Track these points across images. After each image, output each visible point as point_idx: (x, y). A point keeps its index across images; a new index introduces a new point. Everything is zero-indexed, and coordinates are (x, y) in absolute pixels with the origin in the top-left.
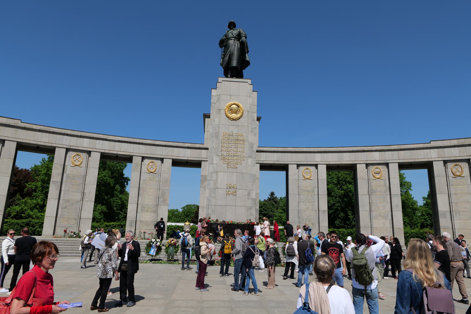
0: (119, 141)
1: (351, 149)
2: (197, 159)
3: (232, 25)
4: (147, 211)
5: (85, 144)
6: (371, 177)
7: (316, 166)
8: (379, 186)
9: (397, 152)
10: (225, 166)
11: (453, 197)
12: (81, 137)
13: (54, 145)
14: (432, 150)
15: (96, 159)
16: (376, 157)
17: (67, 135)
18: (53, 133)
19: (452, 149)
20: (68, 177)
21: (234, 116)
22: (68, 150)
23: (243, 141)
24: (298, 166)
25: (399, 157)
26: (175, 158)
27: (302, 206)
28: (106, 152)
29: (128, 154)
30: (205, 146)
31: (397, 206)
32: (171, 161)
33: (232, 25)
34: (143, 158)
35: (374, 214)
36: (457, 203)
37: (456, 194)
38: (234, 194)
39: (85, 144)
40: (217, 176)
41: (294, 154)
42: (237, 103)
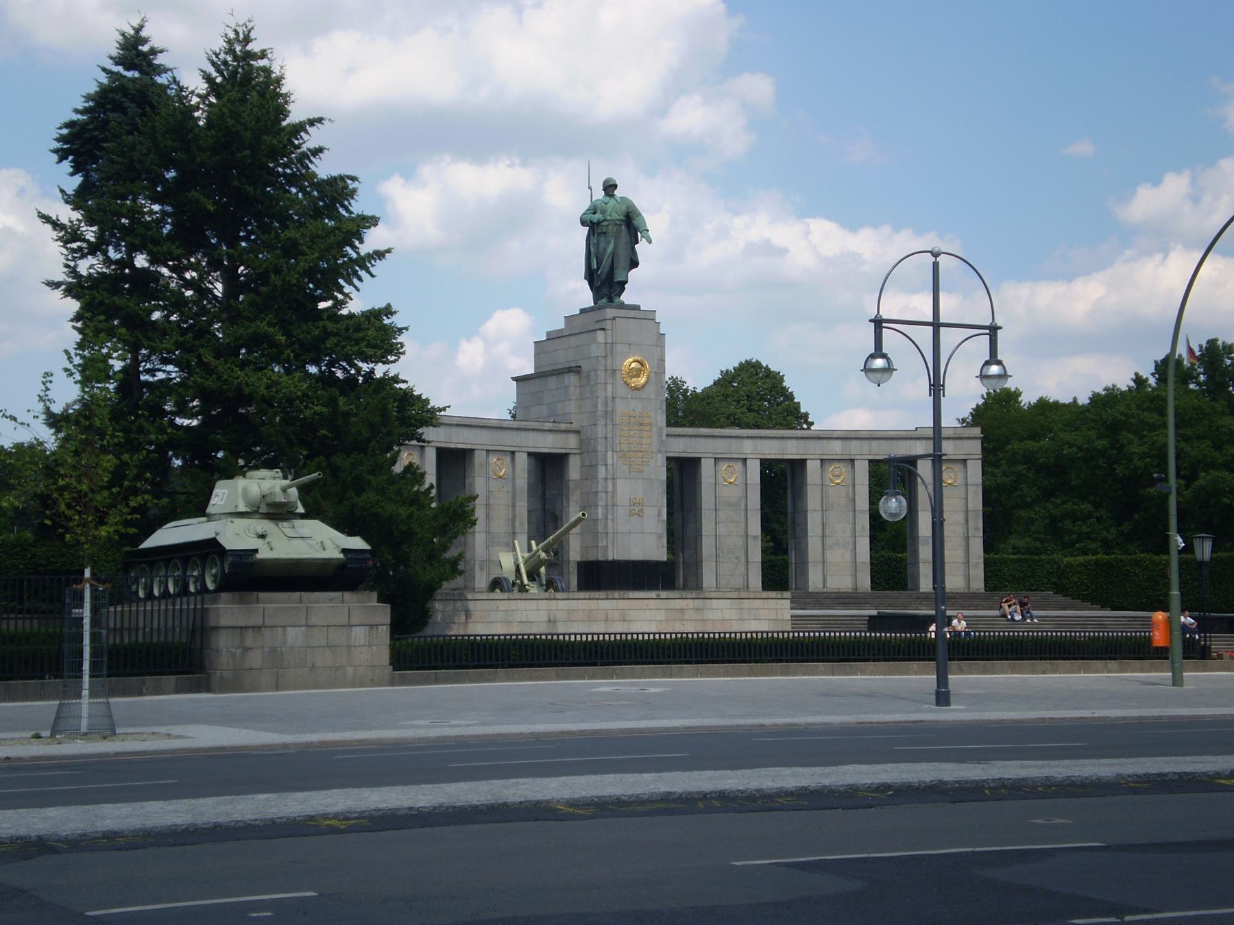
3: (610, 188)
7: (745, 459)
9: (867, 442)
10: (626, 468)
16: (836, 448)
23: (650, 424)
26: (531, 450)
27: (722, 530)
28: (443, 445)
29: (469, 447)
30: (575, 426)
31: (863, 528)
33: (610, 188)
35: (829, 541)
38: (640, 514)
40: (614, 485)
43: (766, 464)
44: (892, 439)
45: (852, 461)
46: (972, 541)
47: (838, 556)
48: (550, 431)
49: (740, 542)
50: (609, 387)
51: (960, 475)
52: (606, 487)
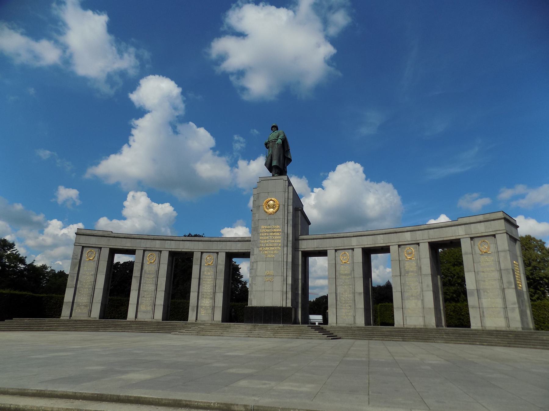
0: (183, 241)
1: (384, 231)
2: (246, 251)
4: (206, 298)
5: (157, 245)
7: (353, 249)
12: (154, 239)
13: (134, 248)
15: (165, 256)
16: (408, 237)
17: (144, 239)
18: (134, 238)
20: (145, 272)
21: (271, 210)
22: (144, 251)
24: (336, 250)
26: (228, 251)
29: (190, 250)
31: (428, 286)
32: (224, 254)
34: (202, 253)
35: (406, 295)
37: (483, 272)
39: (157, 245)
40: (257, 264)
42: (273, 199)
44: (442, 227)
45: (418, 244)
46: (507, 291)
48: (239, 241)
49: (351, 296)
50: (257, 215)
51: (492, 246)
52: (253, 266)
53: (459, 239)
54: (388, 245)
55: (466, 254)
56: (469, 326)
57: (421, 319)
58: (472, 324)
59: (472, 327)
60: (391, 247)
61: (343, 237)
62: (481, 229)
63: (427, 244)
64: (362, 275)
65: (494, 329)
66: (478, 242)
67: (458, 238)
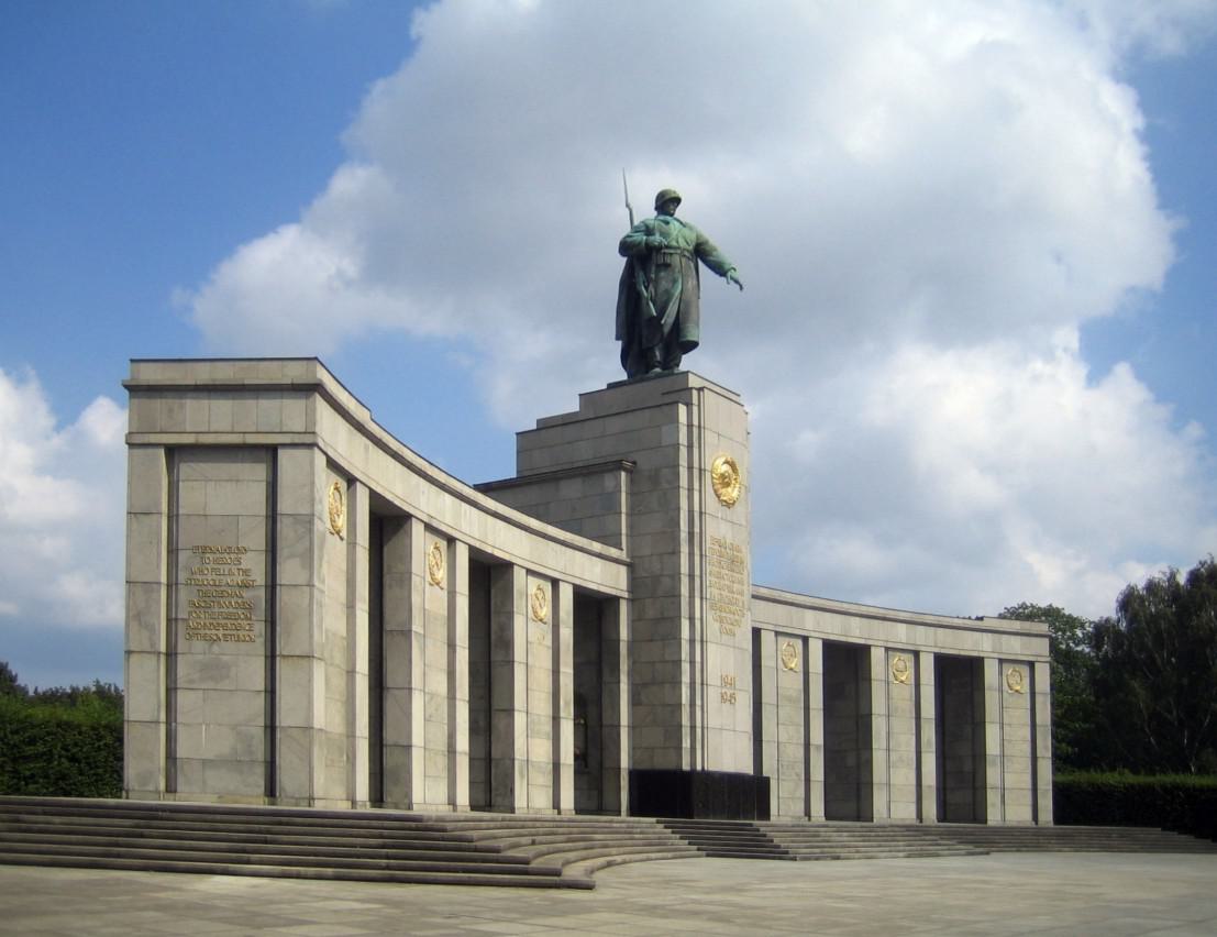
6: (891, 678)
8: (903, 695)
11: (1006, 728)
14: (984, 634)
16: (901, 634)
19: (1013, 637)
25: (936, 643)
26: (578, 582)
35: (894, 757)
36: (1010, 741)
37: (1010, 725)
41: (771, 604)
43: (831, 648)
47: (904, 777)
51: (1027, 681)
53: (983, 658)
54: (869, 642)
55: (990, 689)
56: (985, 821)
57: (913, 808)
58: (989, 818)
59: (990, 823)
60: (873, 650)
61: (792, 604)
62: (1015, 647)
63: (932, 657)
64: (821, 706)
65: (1015, 824)
66: (1008, 669)
67: (982, 655)
